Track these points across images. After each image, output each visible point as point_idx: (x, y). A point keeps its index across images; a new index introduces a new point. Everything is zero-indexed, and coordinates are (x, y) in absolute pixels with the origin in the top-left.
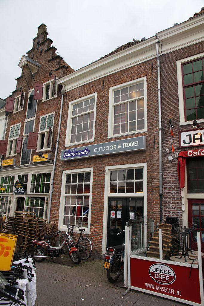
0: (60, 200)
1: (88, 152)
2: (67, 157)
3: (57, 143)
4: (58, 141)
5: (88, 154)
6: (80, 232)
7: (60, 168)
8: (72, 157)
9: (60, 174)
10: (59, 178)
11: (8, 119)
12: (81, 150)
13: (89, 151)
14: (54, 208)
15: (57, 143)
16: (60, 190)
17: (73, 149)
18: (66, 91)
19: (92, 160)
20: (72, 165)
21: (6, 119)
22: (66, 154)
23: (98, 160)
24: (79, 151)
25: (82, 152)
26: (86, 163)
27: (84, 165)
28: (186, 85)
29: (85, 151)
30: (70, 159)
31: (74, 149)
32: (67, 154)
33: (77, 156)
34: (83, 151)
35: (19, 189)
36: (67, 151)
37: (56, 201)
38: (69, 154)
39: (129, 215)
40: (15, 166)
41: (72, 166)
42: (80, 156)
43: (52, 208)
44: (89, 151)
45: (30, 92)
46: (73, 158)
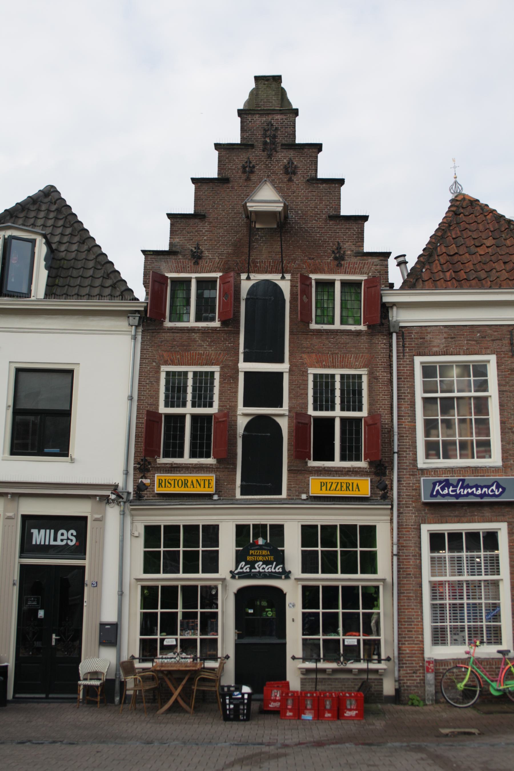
0: (422, 590)
1: (500, 490)
2: (443, 496)
3: (396, 456)
4: (396, 450)
5: (503, 495)
6: (500, 656)
7: (411, 518)
8: (458, 496)
9: (412, 531)
10: (411, 540)
11: (139, 338)
12: (482, 485)
13: (504, 489)
14: (407, 609)
15: (396, 456)
16: (419, 567)
17: (459, 480)
18: (402, 324)
19: (503, 507)
20: (447, 513)
21: (135, 338)
22: (437, 488)
23: (496, 507)
24: (477, 487)
25: (485, 490)
26: (487, 512)
27: (482, 515)
28: (355, 227)
29: (494, 488)
30: (454, 500)
31: (463, 481)
32: (443, 489)
33: (472, 496)
34: (488, 487)
35: (261, 563)
36: (440, 482)
37: (410, 593)
38: (448, 488)
39: (251, 613)
40: (216, 497)
41: (450, 516)
42: (482, 496)
43: (401, 609)
44: (504, 489)
45: (248, 278)
46: (460, 500)
